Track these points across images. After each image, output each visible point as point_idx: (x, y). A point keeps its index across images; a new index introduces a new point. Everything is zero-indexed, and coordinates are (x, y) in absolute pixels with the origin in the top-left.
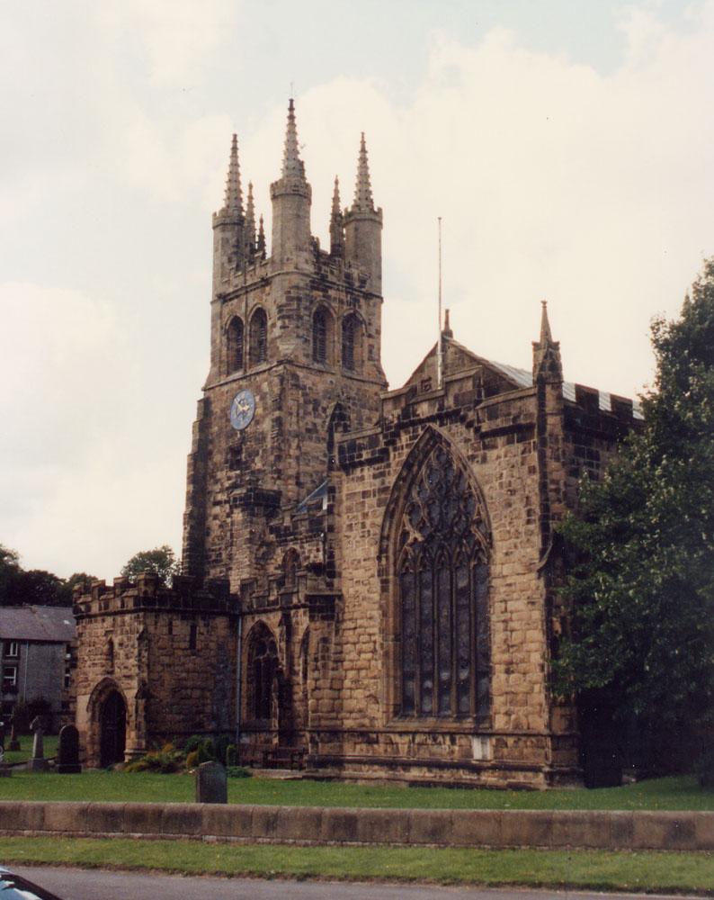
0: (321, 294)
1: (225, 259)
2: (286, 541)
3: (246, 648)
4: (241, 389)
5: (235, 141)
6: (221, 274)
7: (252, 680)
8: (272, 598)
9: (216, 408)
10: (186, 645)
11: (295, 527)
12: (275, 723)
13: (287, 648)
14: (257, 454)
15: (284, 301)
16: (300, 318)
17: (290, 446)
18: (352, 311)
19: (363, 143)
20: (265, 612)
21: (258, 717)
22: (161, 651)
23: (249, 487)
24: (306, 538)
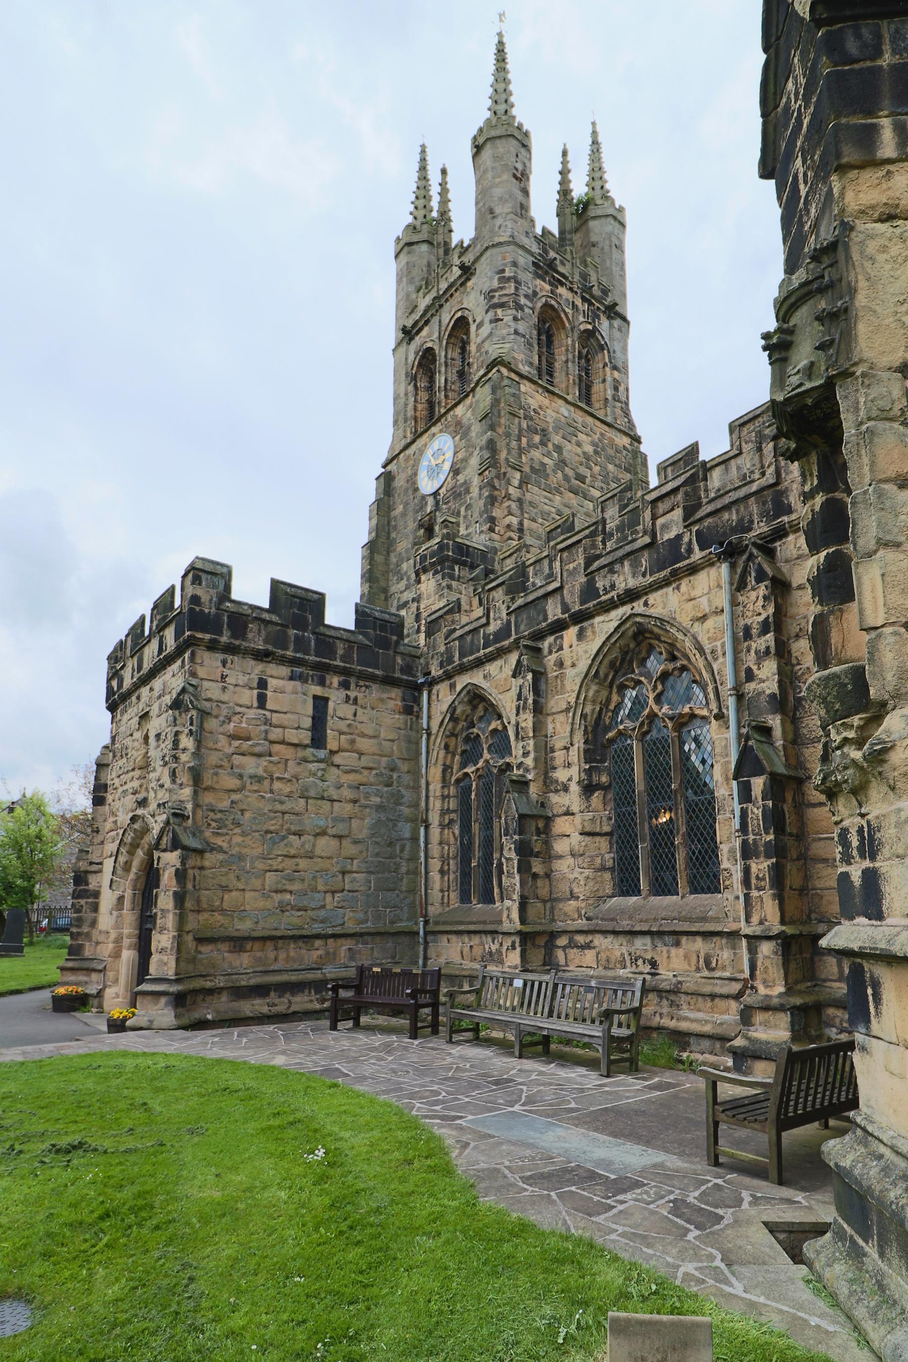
0: (548, 287)
1: (412, 289)
3: (438, 754)
5: (423, 151)
6: (407, 306)
7: (451, 821)
9: (400, 482)
10: (305, 737)
12: (511, 918)
13: (538, 727)
15: (495, 284)
16: (519, 307)
17: (509, 483)
18: (590, 327)
19: (594, 133)
20: (479, 663)
21: (465, 897)
22: (236, 743)
23: (445, 531)
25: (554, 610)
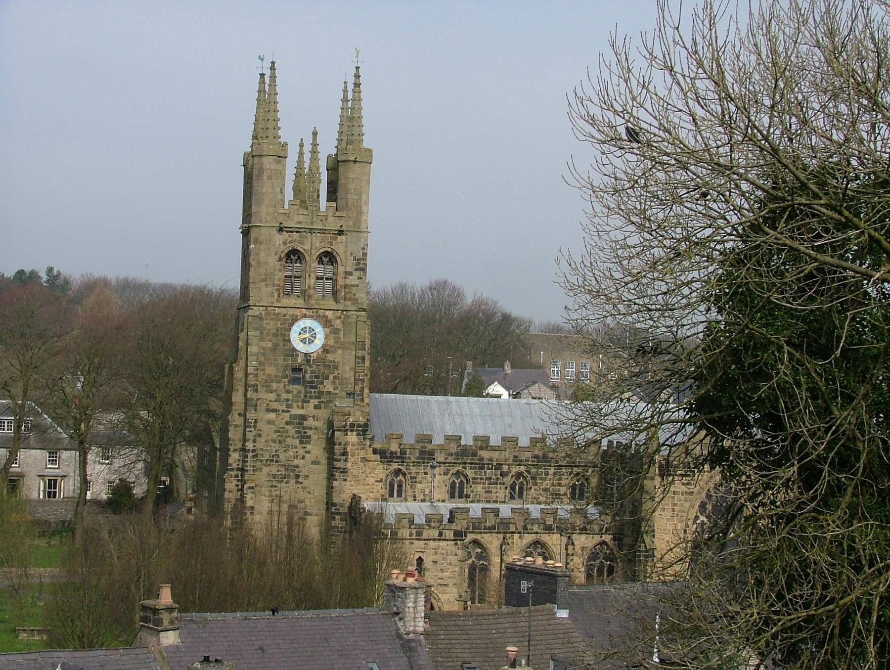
2: (391, 461)
4: (305, 316)
8: (488, 524)
11: (403, 452)
14: (327, 378)
20: (481, 533)
24: (414, 462)
25: (512, 528)
